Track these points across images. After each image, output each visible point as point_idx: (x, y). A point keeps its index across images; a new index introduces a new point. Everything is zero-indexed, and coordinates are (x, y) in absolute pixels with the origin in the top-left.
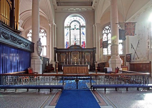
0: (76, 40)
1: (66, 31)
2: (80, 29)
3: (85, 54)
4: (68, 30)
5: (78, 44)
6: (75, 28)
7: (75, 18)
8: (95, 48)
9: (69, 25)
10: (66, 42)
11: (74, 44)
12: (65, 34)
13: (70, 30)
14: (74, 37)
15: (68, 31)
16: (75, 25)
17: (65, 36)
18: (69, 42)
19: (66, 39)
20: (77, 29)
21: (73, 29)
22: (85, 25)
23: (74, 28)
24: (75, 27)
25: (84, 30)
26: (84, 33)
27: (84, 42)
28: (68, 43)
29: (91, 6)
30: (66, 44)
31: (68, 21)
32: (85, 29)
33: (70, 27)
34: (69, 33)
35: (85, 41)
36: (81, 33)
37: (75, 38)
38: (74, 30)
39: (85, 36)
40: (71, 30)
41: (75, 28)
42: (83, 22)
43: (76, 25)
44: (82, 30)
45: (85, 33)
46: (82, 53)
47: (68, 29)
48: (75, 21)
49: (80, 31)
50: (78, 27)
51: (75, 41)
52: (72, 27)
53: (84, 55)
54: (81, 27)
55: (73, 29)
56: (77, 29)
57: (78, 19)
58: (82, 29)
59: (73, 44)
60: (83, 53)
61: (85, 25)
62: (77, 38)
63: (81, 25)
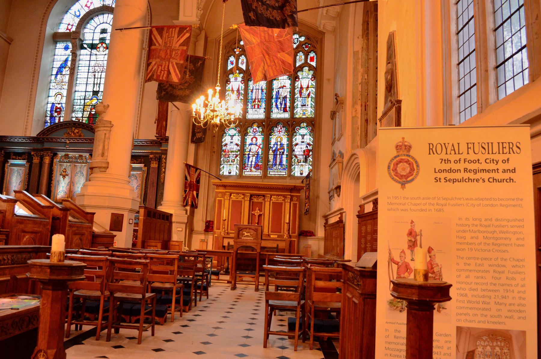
4: (66, 48)
10: (52, 108)
11: (86, 114)
13: (74, 55)
21: (93, 47)
34: (69, 63)
37: (96, 89)
38: (94, 51)
41: (102, 40)
59: (80, 115)
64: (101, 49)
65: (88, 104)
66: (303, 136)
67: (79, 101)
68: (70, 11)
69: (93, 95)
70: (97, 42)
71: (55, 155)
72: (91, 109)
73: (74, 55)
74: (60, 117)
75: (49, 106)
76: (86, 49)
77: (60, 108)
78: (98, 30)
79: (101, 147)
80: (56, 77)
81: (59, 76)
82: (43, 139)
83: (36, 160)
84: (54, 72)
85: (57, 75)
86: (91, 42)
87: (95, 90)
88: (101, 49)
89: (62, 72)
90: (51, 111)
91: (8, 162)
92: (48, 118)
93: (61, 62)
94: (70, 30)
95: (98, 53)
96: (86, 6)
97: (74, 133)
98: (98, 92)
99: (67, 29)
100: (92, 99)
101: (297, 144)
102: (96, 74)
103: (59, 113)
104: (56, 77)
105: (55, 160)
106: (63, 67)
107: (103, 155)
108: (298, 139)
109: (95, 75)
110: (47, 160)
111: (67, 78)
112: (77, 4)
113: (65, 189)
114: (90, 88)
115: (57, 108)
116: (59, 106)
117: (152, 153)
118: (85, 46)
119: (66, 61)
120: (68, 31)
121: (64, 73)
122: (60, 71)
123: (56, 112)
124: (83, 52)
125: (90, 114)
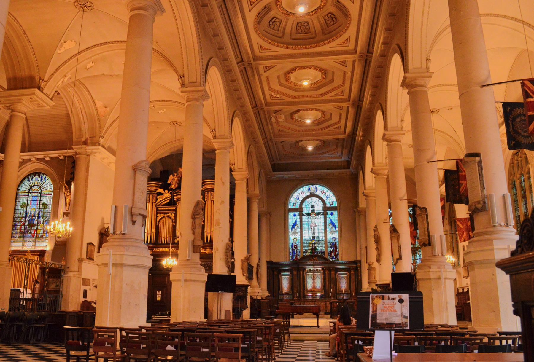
0: (316, 239)
1: (292, 218)
2: (325, 214)
3: (336, 273)
4: (295, 215)
5: (320, 248)
6: (313, 211)
7: (312, 188)
8: (360, 261)
9: (298, 206)
10: (292, 245)
11: (311, 248)
12: (290, 227)
13: (301, 219)
14: (310, 231)
15: (295, 217)
16: (313, 204)
17: (290, 230)
18: (299, 245)
19: (293, 237)
20: (318, 214)
21: (308, 214)
22: (335, 204)
23: (310, 212)
24: (312, 209)
25: (335, 217)
26: (334, 222)
27: (334, 245)
28: (296, 247)
29: (349, 168)
30: (293, 250)
31: (295, 199)
32: (336, 213)
33: (300, 210)
34: (298, 223)
35: (337, 240)
36: (328, 222)
37: (314, 235)
38: (310, 217)
39: (337, 229)
40: (303, 217)
42: (331, 198)
43: (316, 206)
44: (331, 216)
45: (336, 223)
46: (330, 271)
47: (297, 213)
48: (312, 195)
49: (325, 218)
50: (319, 208)
51: (314, 242)
52: (306, 209)
53: (335, 275)
54: (326, 209)
55: (308, 214)
56: (318, 214)
57: (319, 189)
58: (329, 213)
59: (307, 248)
60: (333, 272)
61: (335, 204)
62: (317, 235)
63: (328, 205)
64: (313, 215)
65: (310, 243)
66: (420, 255)
67: (306, 242)
68: (293, 196)
69: (312, 238)
70: (311, 212)
71: (305, 269)
72: (313, 246)
73: (301, 219)
74: (297, 250)
75: (290, 245)
76: (305, 215)
77: (296, 245)
78: (310, 206)
79: (373, 276)
80: (292, 230)
81: (293, 230)
82: (300, 263)
83: (295, 273)
84: (290, 227)
85: (292, 229)
86: (307, 212)
87: (313, 236)
88: (313, 215)
89: (294, 227)
90: (292, 247)
91: (281, 274)
92: (291, 251)
93: (293, 223)
94: (295, 206)
95: (312, 218)
96: (301, 193)
97: (314, 259)
98: (315, 237)
99: (294, 206)
100: (312, 240)
101: (417, 259)
102: (312, 228)
103: (296, 248)
104: (292, 230)
105: (305, 272)
106: (294, 225)
107: (374, 279)
108: (418, 256)
109: (312, 229)
110: (301, 273)
111: (298, 231)
112: (296, 192)
113: (311, 285)
114: (311, 235)
115: (295, 245)
116: (296, 244)
117: (350, 267)
118: (305, 214)
119: (296, 222)
120: (294, 207)
121: (295, 228)
122: (293, 227)
123: (294, 247)
124: (303, 217)
125: (312, 248)
